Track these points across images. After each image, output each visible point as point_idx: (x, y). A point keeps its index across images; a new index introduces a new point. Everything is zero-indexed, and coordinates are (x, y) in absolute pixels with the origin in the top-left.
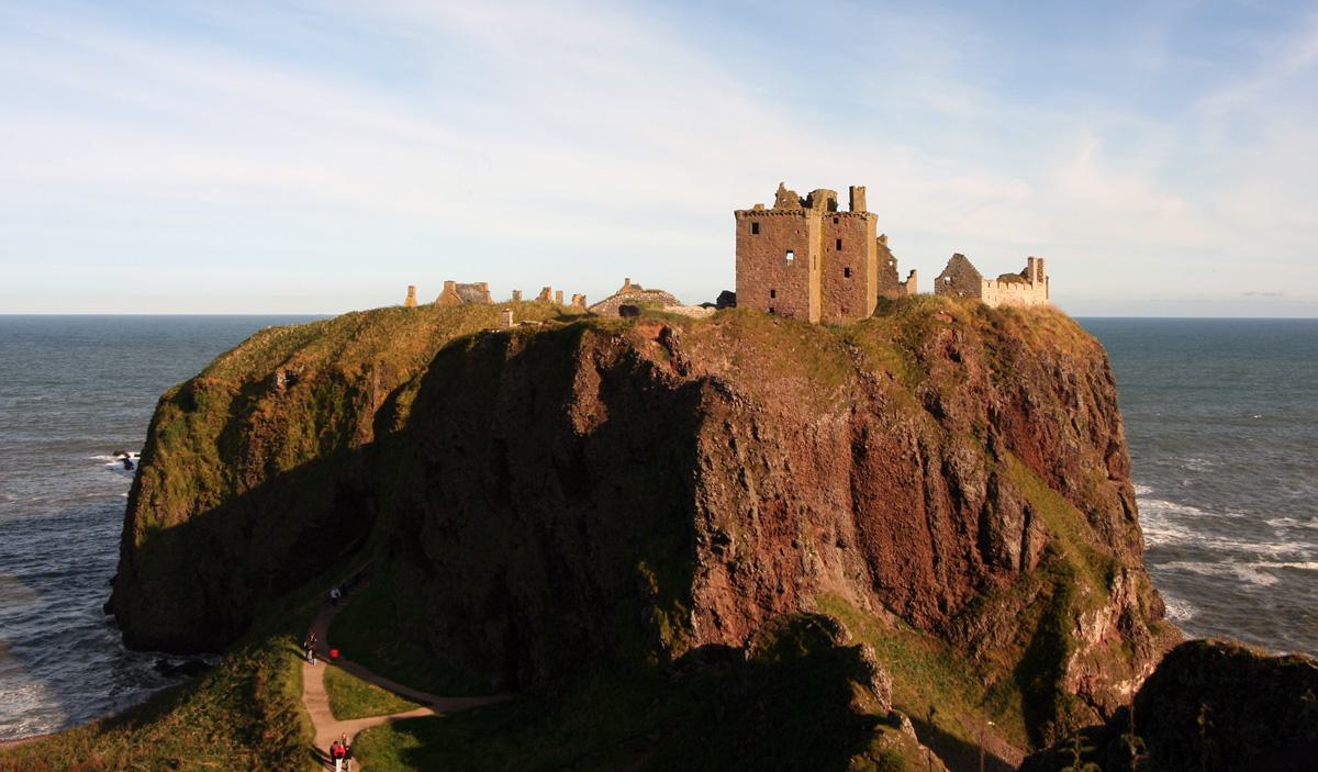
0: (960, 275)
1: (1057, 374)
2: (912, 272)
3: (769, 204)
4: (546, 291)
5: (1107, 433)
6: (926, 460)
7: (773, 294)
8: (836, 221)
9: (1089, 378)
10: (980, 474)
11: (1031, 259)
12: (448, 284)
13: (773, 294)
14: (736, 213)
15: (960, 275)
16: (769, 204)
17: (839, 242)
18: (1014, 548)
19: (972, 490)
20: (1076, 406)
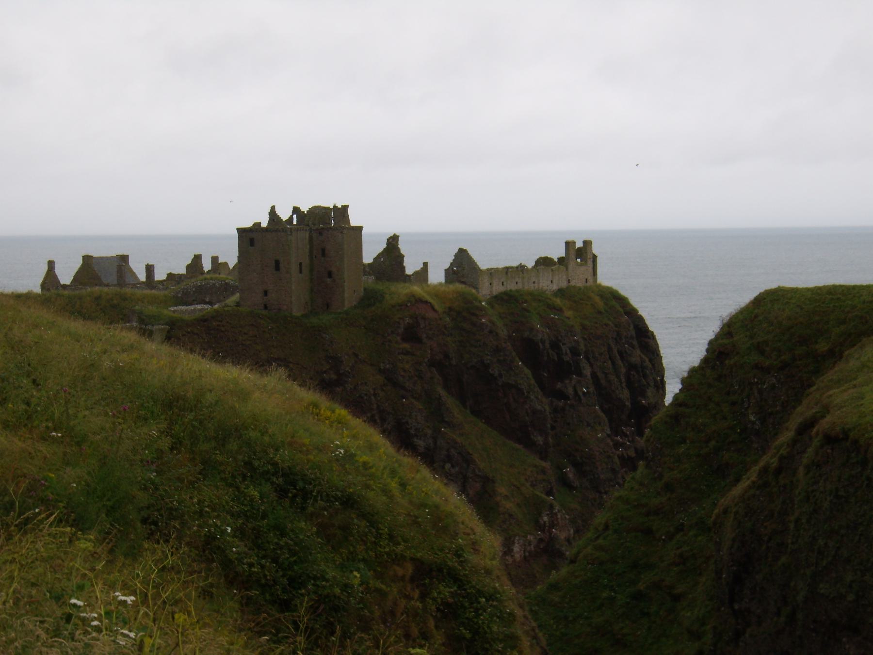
0: (462, 265)
1: (555, 345)
2: (425, 264)
3: (264, 224)
4: (197, 258)
5: (625, 394)
7: (266, 293)
8: (321, 234)
9: (610, 349)
10: (429, 432)
11: (569, 245)
12: (87, 259)
13: (266, 293)
14: (242, 232)
15: (462, 265)
16: (264, 224)
17: (323, 250)
20: (580, 374)
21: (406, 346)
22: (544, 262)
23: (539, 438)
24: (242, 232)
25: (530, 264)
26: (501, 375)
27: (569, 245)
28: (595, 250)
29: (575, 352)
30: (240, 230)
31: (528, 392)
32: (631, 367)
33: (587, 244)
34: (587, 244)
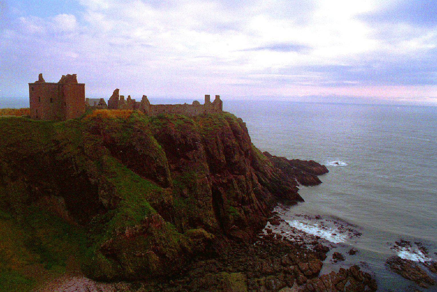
1: (184, 137)
6: (77, 170)
18: (105, 201)
19: (93, 181)
20: (197, 150)
21: (92, 136)
22: (196, 103)
23: (162, 178)
24: (30, 85)
25: (191, 104)
26: (141, 151)
27: (207, 97)
28: (221, 98)
29: (194, 140)
30: (30, 85)
31: (156, 159)
32: (228, 147)
33: (217, 97)
34: (217, 97)
